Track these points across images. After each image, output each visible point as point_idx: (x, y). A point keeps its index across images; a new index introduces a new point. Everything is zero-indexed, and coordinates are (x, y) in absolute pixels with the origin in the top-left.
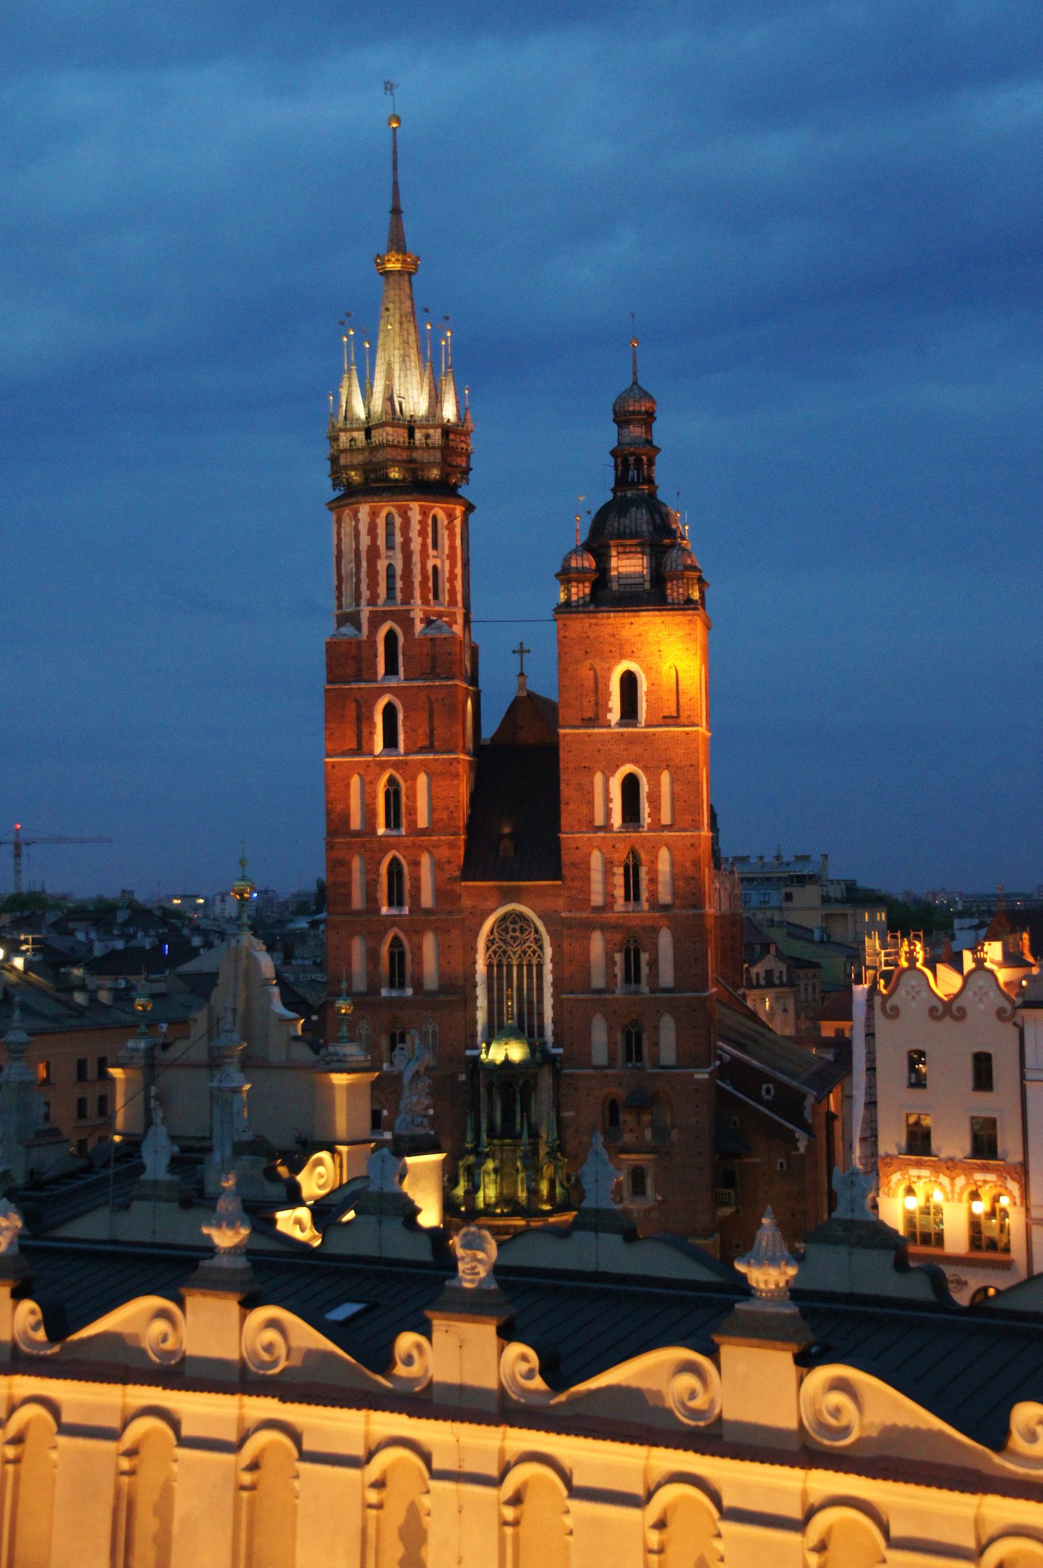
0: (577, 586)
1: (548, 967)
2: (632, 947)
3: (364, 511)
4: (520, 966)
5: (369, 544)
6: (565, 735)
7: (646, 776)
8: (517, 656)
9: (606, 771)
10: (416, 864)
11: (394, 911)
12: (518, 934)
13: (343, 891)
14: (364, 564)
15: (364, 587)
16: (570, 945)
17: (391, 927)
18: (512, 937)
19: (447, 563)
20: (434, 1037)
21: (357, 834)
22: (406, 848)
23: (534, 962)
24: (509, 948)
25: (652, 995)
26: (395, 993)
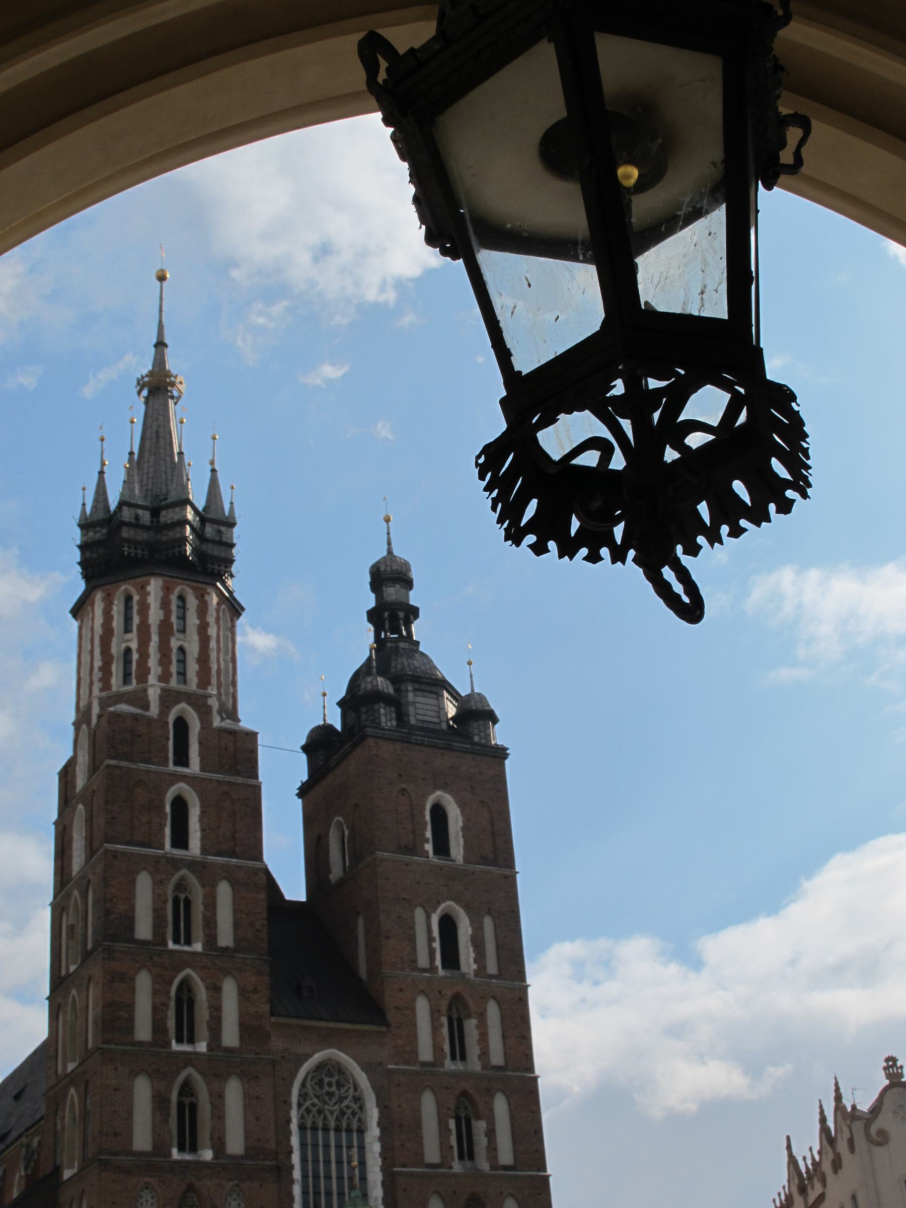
0: (385, 708)
2: (463, 1115)
3: (154, 586)
4: (338, 1130)
5: (162, 618)
6: (382, 861)
7: (469, 917)
10: (215, 989)
11: (185, 1048)
12: (334, 1088)
13: (122, 1013)
14: (155, 638)
15: (153, 662)
16: (400, 1106)
21: (144, 943)
23: (355, 1125)
24: (327, 1107)
25: (493, 1172)
26: (188, 1157)
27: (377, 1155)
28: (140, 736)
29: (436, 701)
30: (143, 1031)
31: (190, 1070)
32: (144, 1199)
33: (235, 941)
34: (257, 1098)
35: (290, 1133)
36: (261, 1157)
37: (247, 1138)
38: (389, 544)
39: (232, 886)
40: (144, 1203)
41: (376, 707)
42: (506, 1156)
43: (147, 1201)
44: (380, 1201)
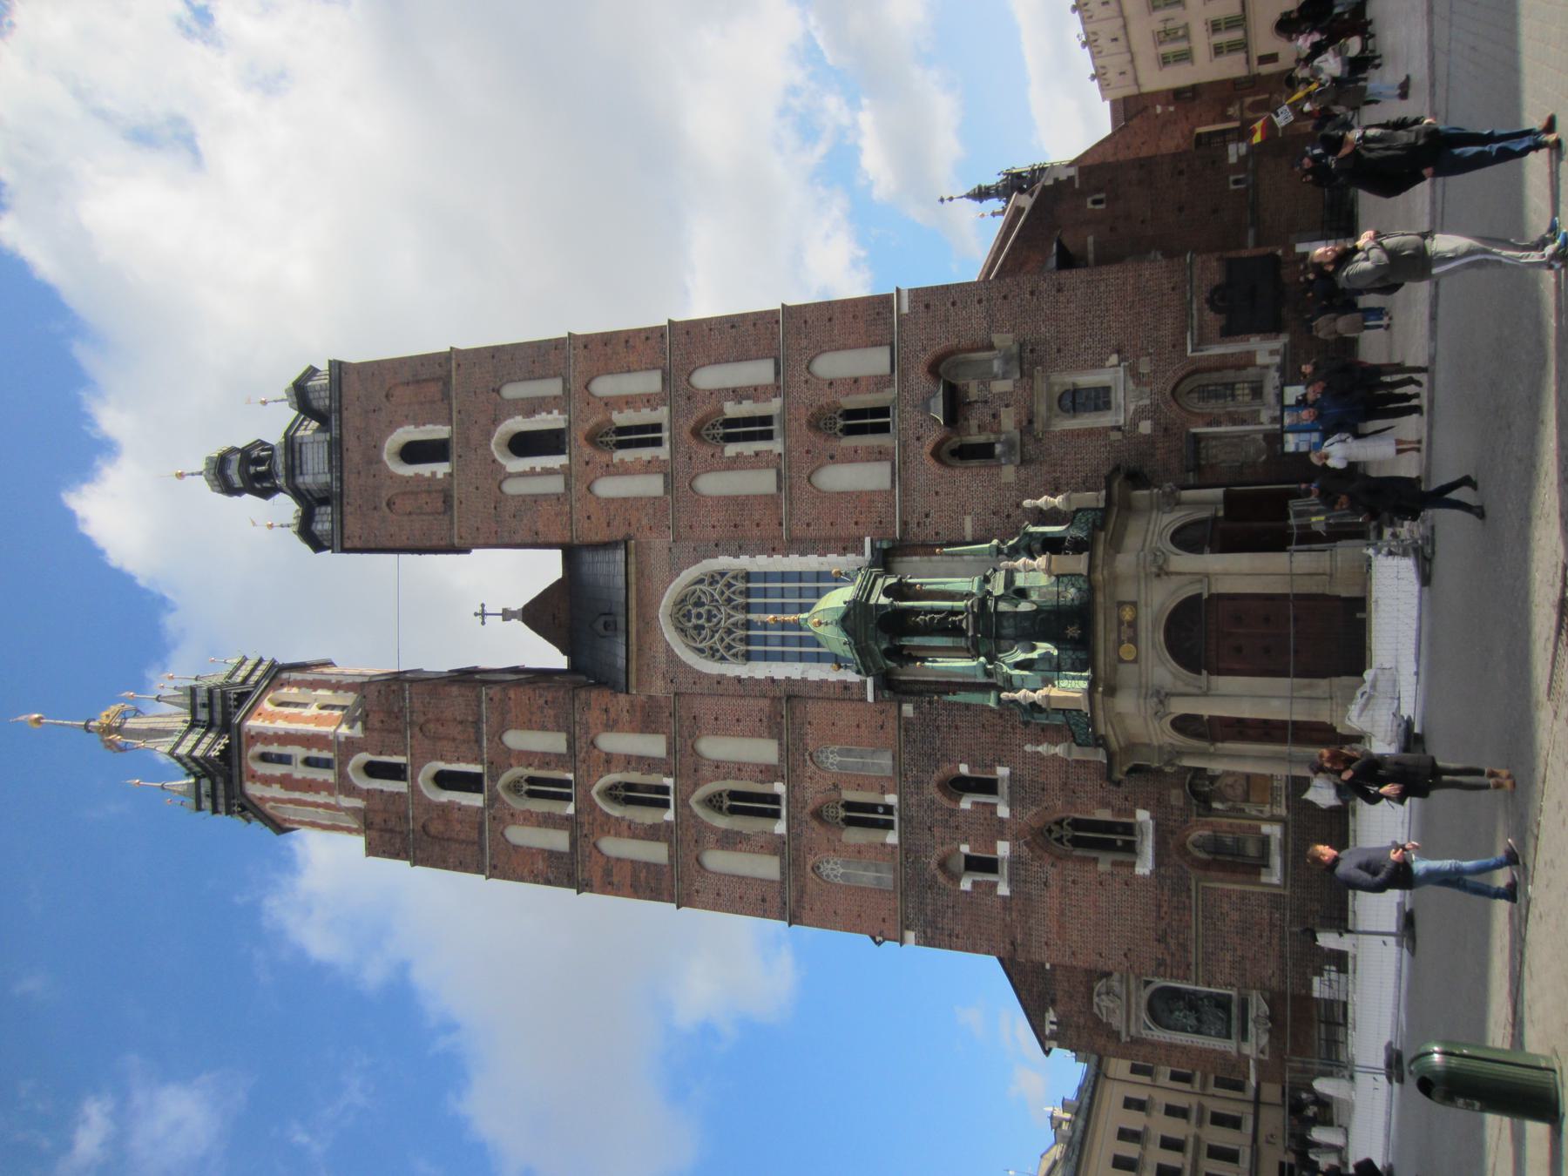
1: (745, 563)
2: (722, 431)
4: (748, 608)
7: (505, 420)
8: (488, 619)
9: (499, 478)
10: (609, 760)
12: (702, 610)
13: (643, 875)
14: (297, 795)
16: (714, 527)
17: (690, 806)
18: (709, 620)
19: (320, 692)
20: (848, 753)
22: (589, 775)
23: (740, 585)
27: (771, 559)
28: (385, 821)
29: (310, 446)
30: (657, 852)
31: (692, 802)
32: (829, 871)
33: (558, 731)
34: (716, 719)
35: (751, 678)
36: (779, 720)
37: (760, 736)
38: (201, 473)
39: (507, 730)
40: (835, 872)
41: (317, 533)
42: (760, 372)
43: (832, 869)
44: (822, 559)
